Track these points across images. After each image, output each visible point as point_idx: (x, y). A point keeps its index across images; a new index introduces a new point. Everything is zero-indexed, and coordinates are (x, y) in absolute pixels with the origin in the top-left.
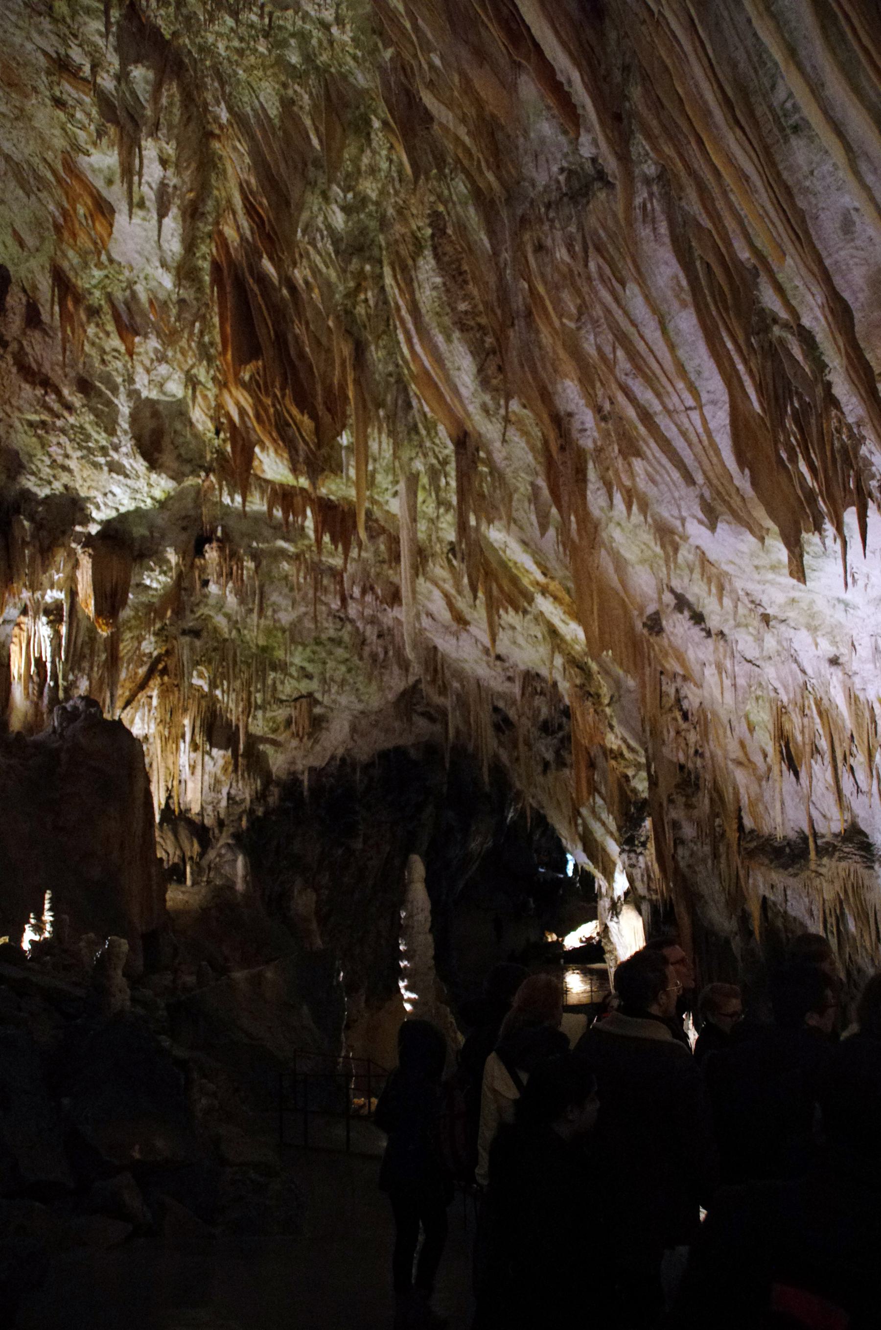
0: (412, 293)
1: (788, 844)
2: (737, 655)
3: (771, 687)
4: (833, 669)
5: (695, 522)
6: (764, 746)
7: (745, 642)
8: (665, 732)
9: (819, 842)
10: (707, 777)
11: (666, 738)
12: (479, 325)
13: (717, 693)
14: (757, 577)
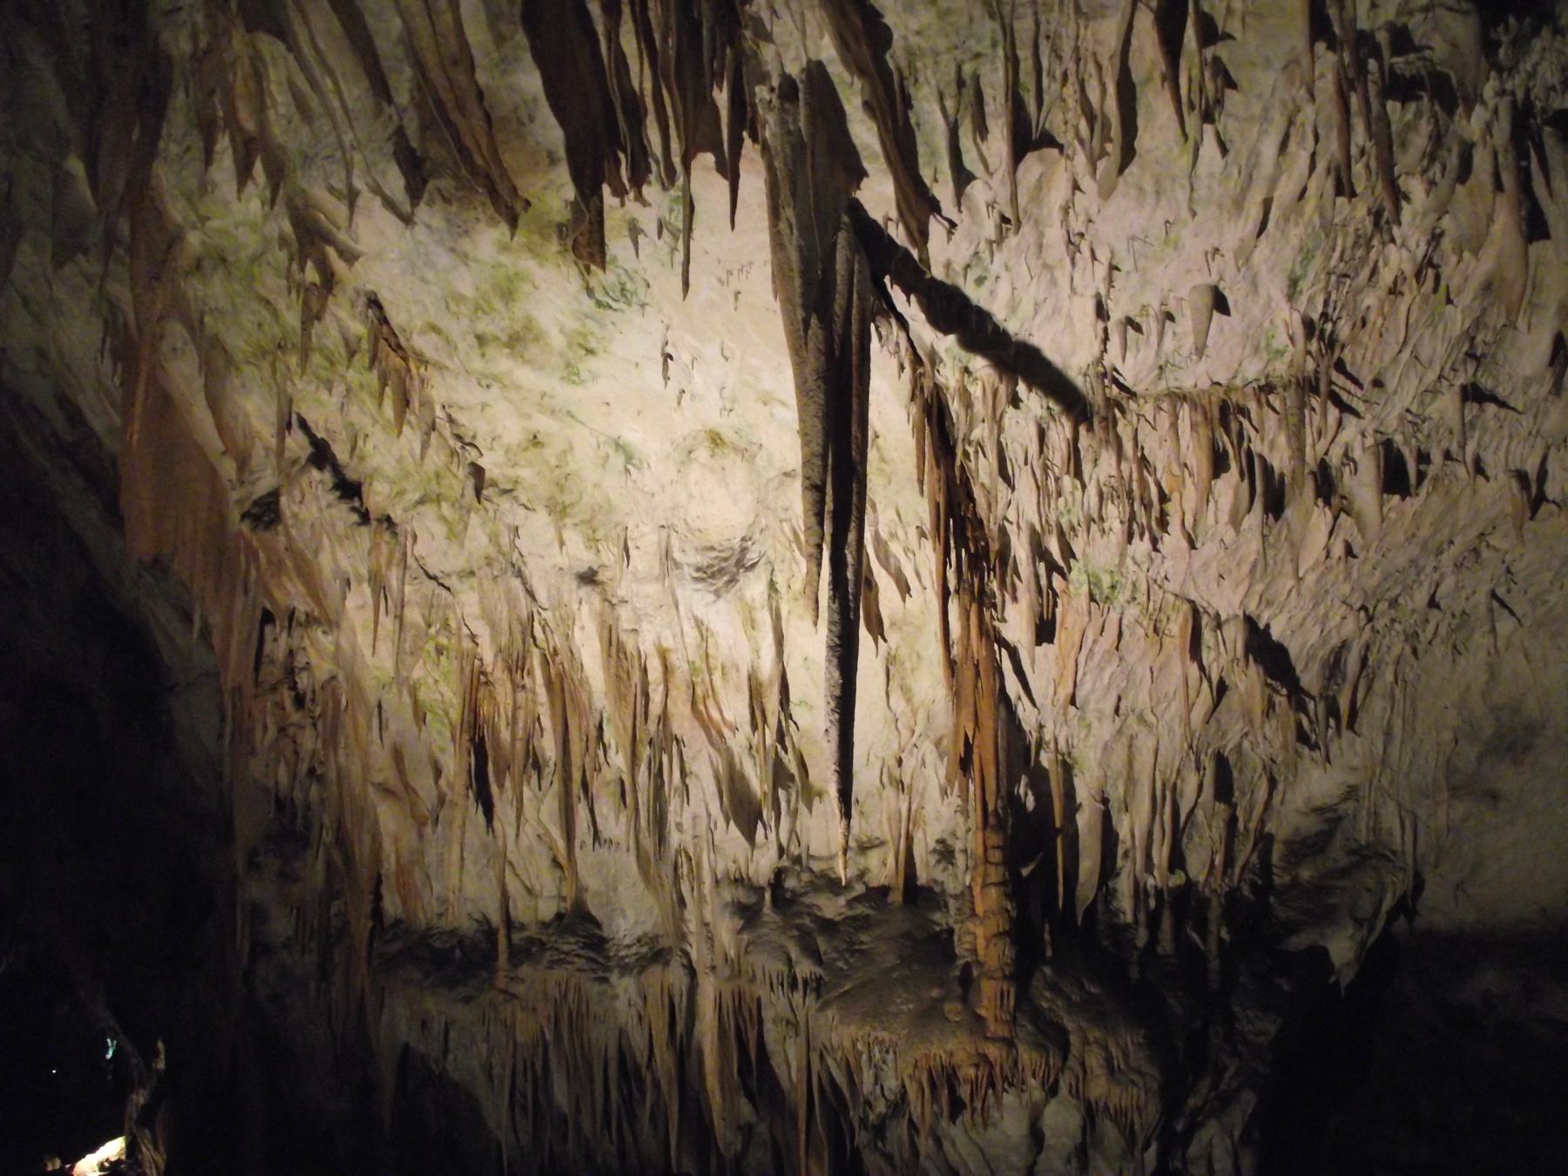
1: (460, 942)
2: (410, 561)
3: (465, 631)
4: (585, 591)
6: (437, 752)
7: (430, 540)
8: (259, 733)
9: (516, 937)
10: (326, 820)
11: (258, 744)
13: (364, 641)
14: (477, 364)
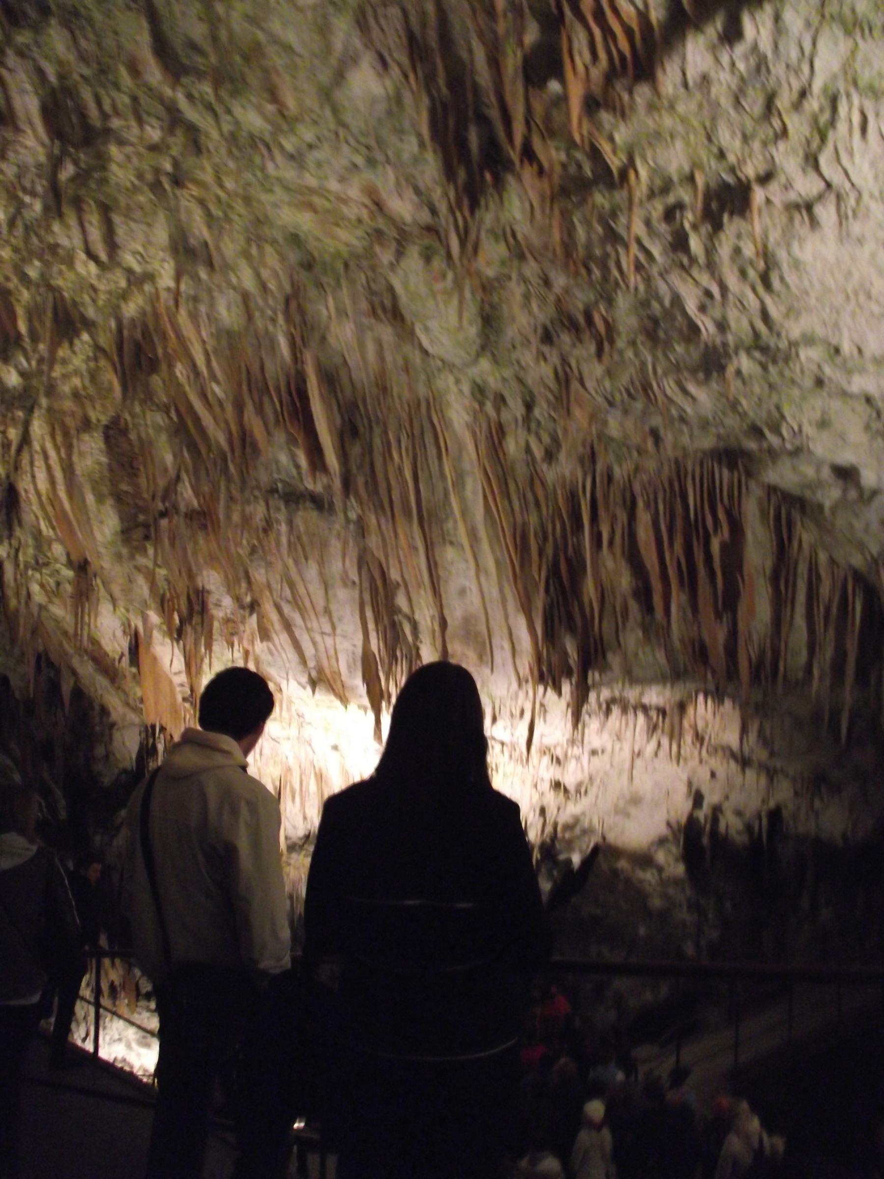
0: (69, 455)
4: (334, 752)
5: (295, 683)
12: (136, 504)
